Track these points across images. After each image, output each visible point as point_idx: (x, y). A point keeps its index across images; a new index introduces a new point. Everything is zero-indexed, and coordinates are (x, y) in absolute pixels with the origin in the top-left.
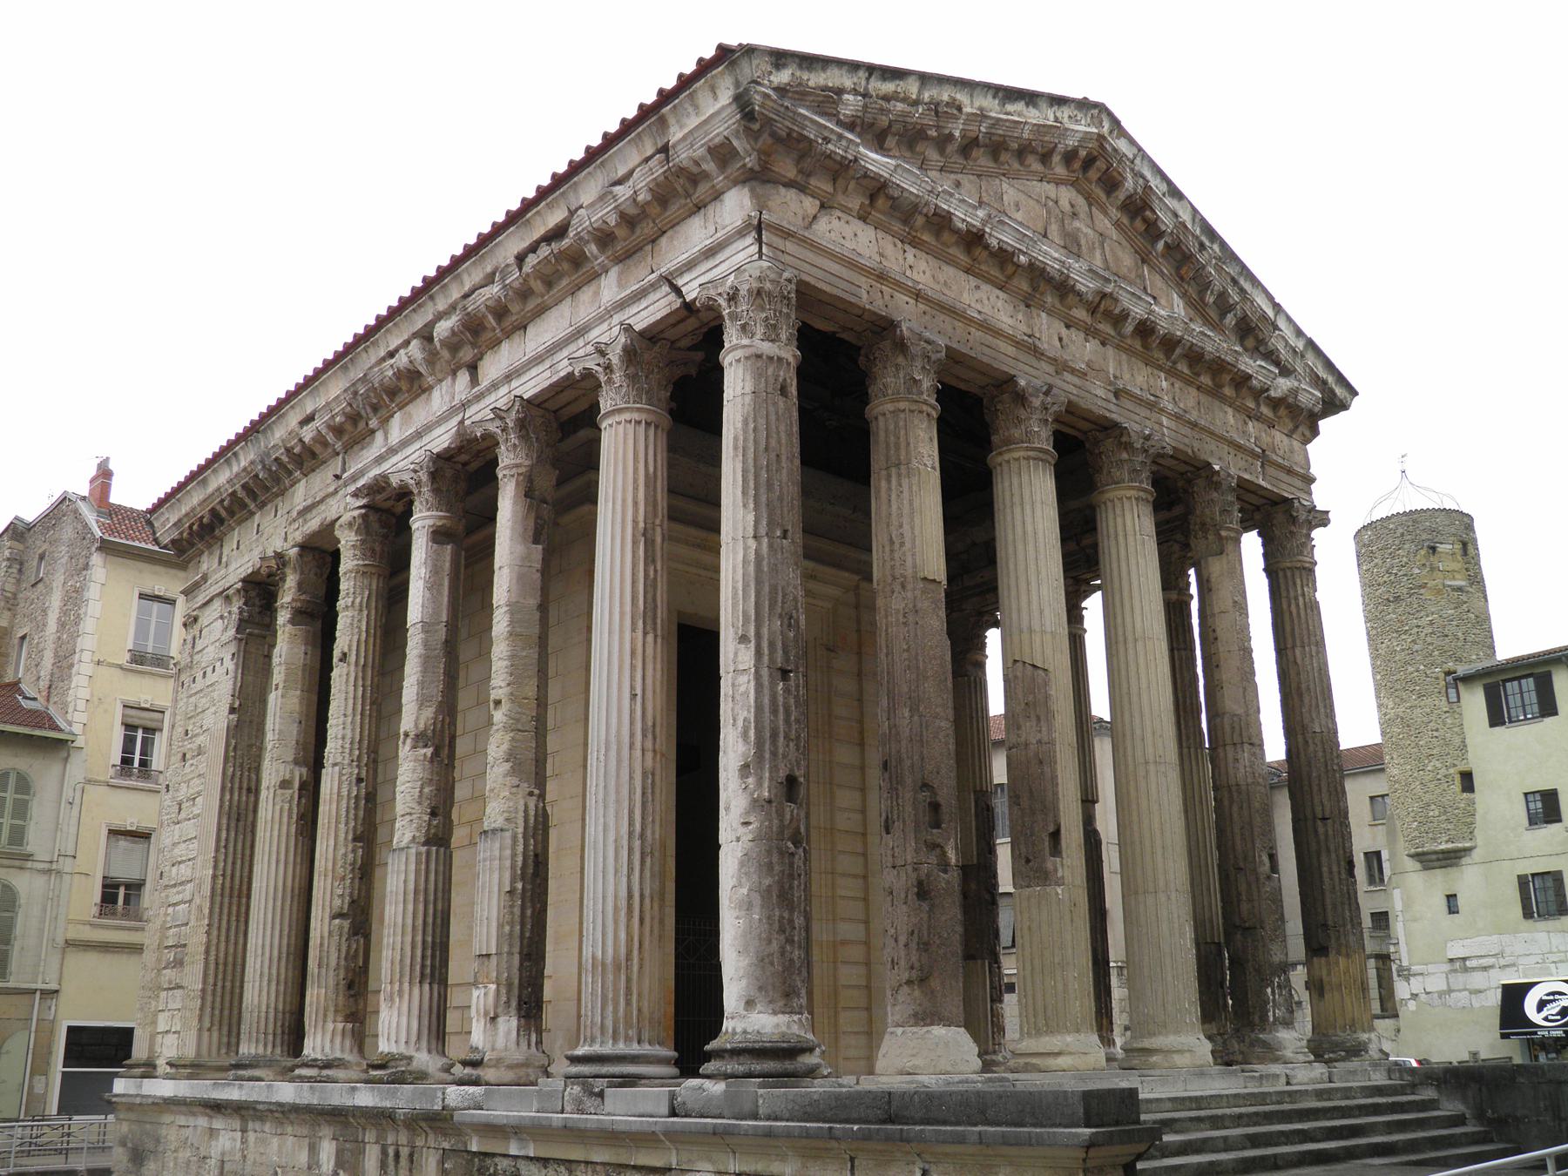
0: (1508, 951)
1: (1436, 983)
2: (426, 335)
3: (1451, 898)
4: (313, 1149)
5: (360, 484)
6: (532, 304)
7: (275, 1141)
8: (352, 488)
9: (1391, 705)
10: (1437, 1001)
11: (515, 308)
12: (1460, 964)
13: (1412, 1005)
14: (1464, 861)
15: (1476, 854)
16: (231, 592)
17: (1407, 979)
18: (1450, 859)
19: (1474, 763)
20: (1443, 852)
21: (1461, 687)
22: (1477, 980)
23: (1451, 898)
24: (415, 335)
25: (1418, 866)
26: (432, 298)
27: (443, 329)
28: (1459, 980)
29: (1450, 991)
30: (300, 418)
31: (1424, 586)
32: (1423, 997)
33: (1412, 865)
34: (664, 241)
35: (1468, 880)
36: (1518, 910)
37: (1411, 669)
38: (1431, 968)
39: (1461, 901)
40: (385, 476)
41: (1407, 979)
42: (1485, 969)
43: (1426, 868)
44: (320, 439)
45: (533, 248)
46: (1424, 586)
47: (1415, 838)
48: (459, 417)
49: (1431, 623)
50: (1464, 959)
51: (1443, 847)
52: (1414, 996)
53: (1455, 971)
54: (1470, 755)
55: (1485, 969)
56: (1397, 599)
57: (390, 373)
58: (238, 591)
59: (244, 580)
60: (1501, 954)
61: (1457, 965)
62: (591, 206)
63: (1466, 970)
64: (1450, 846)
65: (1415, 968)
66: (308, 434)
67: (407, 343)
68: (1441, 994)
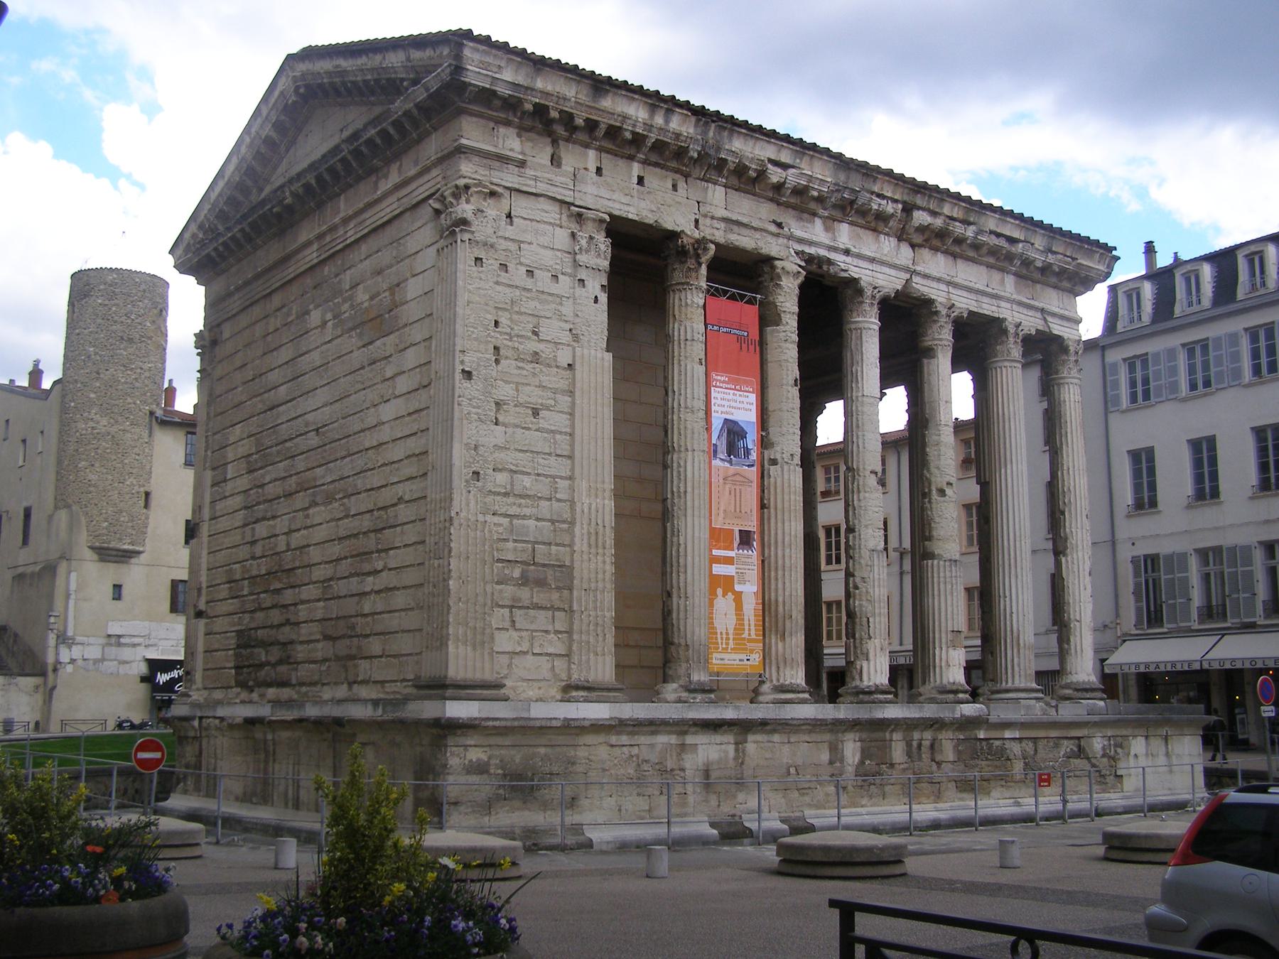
0: (153, 634)
1: (93, 652)
2: (908, 209)
3: (118, 588)
4: (835, 749)
5: (808, 250)
6: (971, 254)
7: (786, 749)
8: (799, 248)
9: (104, 422)
10: (91, 667)
11: (964, 246)
12: (115, 640)
13: (70, 668)
14: (133, 560)
15: (142, 556)
16: (591, 214)
17: (70, 648)
18: (125, 556)
19: (155, 486)
20: (125, 551)
21: (156, 427)
22: (126, 653)
23: (118, 588)
24: (904, 203)
25: (95, 557)
26: (930, 197)
27: (921, 218)
28: (113, 651)
29: (103, 660)
30: (773, 157)
31: (150, 338)
32: (80, 662)
33: (89, 554)
34: (1038, 286)
35: (134, 576)
36: (167, 605)
37: (129, 400)
38: (92, 640)
39: (125, 592)
40: (830, 262)
41: (70, 648)
42: (134, 645)
43: (102, 560)
44: (779, 187)
45: (998, 235)
46: (150, 338)
47: (103, 535)
48: (908, 276)
49: (150, 369)
50: (119, 636)
51: (126, 547)
52: (73, 661)
53: (111, 645)
54: (152, 481)
55: (134, 645)
56: (131, 340)
57: (875, 207)
58: (602, 221)
59: (611, 215)
60: (148, 636)
61: (113, 640)
62: (1036, 248)
63: (119, 645)
64: (131, 547)
65: (79, 639)
66: (775, 175)
67: (896, 201)
68: (96, 661)
